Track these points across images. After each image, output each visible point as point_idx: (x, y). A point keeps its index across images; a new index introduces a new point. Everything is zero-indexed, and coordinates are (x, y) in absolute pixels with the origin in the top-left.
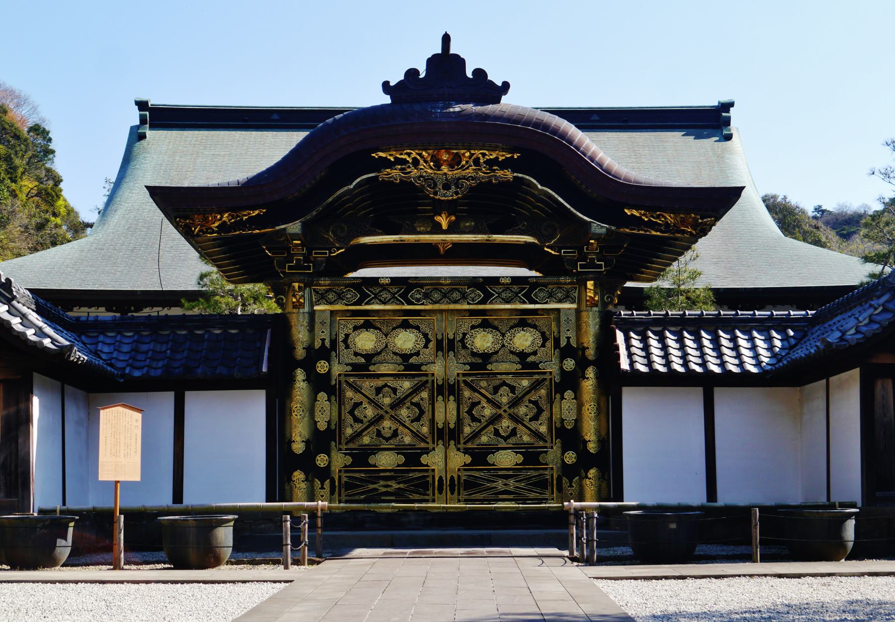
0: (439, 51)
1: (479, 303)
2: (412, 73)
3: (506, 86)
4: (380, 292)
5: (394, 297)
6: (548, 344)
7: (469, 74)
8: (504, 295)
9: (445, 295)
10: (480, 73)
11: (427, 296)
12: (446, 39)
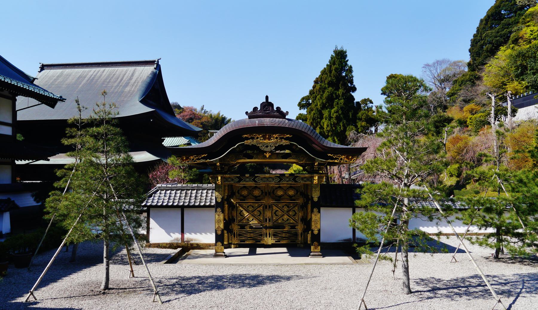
0: (265, 101)
2: (255, 109)
3: (287, 113)
6: (299, 193)
7: (275, 109)
10: (278, 108)
12: (267, 97)
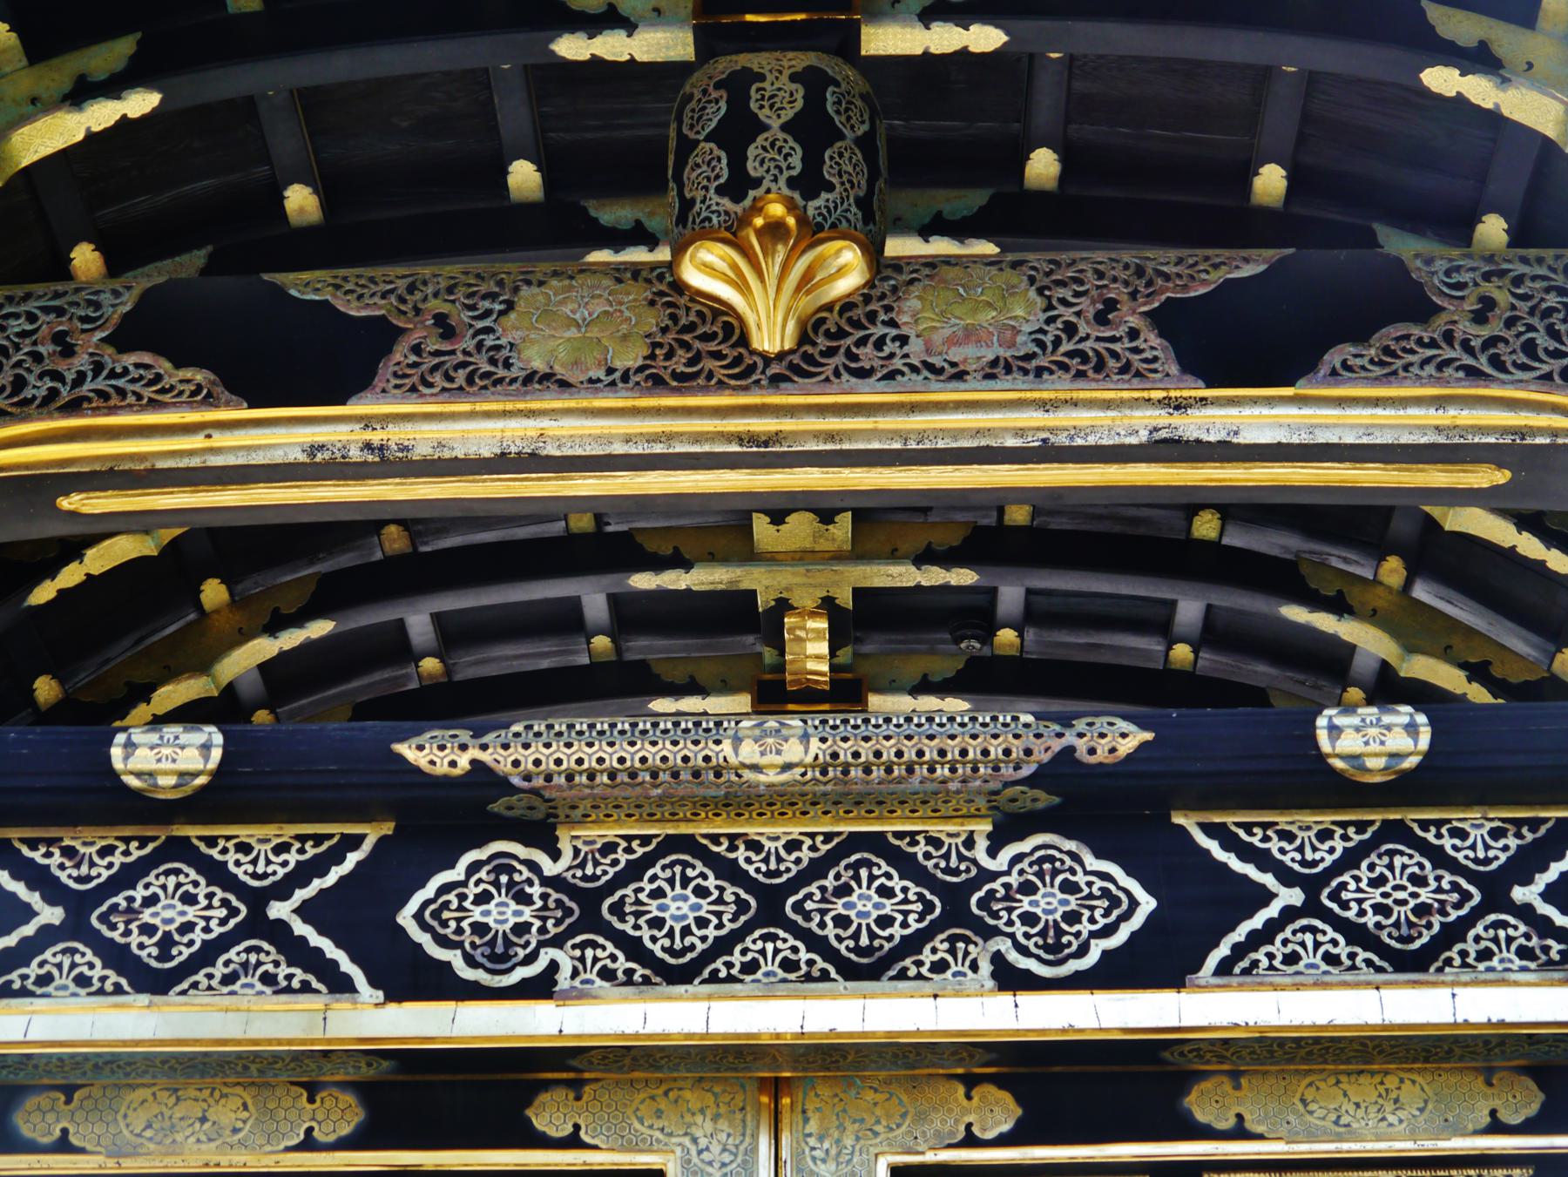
1: (1114, 974)
4: (128, 877)
5: (259, 926)
8: (1359, 894)
9: (770, 905)
11: (585, 909)
